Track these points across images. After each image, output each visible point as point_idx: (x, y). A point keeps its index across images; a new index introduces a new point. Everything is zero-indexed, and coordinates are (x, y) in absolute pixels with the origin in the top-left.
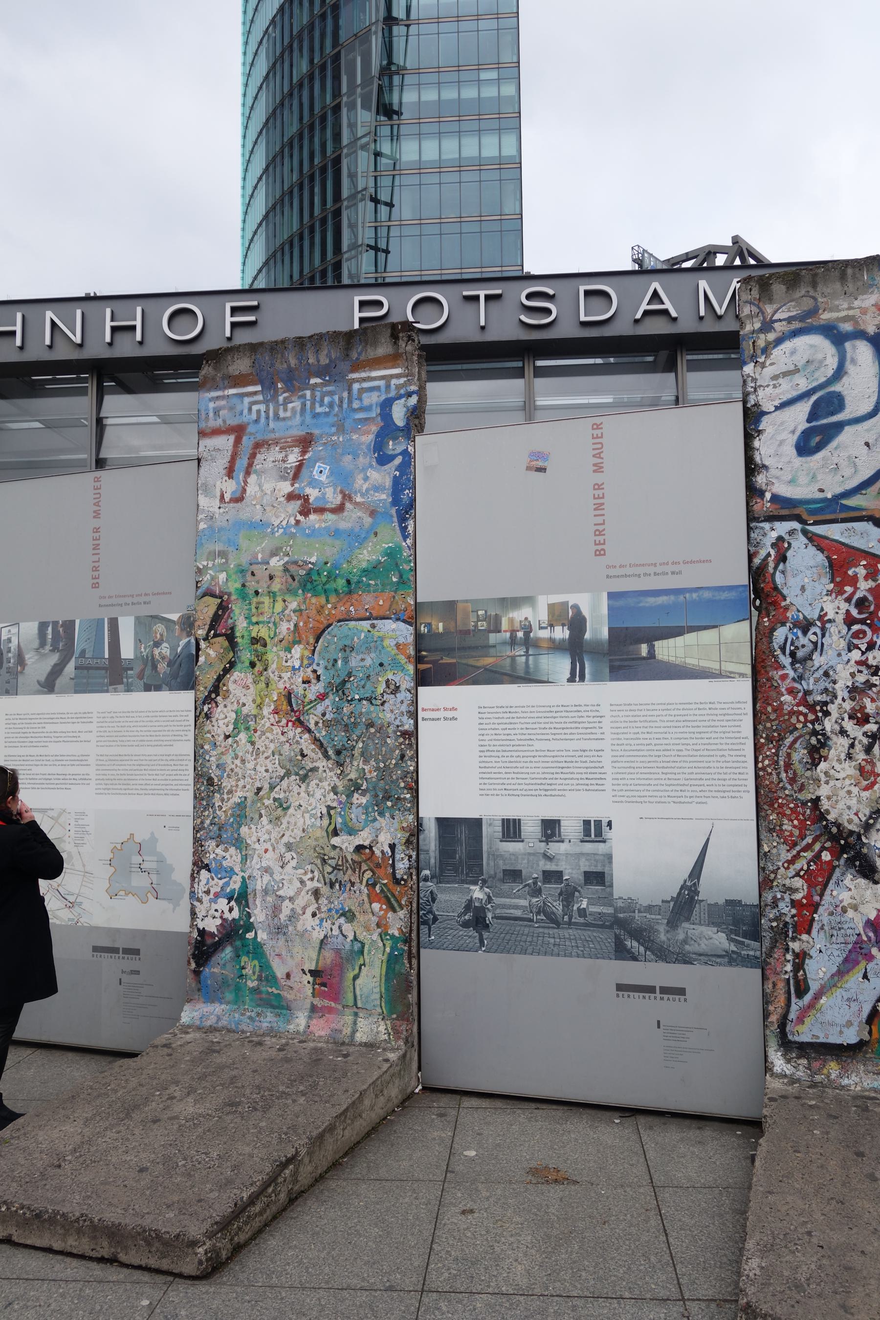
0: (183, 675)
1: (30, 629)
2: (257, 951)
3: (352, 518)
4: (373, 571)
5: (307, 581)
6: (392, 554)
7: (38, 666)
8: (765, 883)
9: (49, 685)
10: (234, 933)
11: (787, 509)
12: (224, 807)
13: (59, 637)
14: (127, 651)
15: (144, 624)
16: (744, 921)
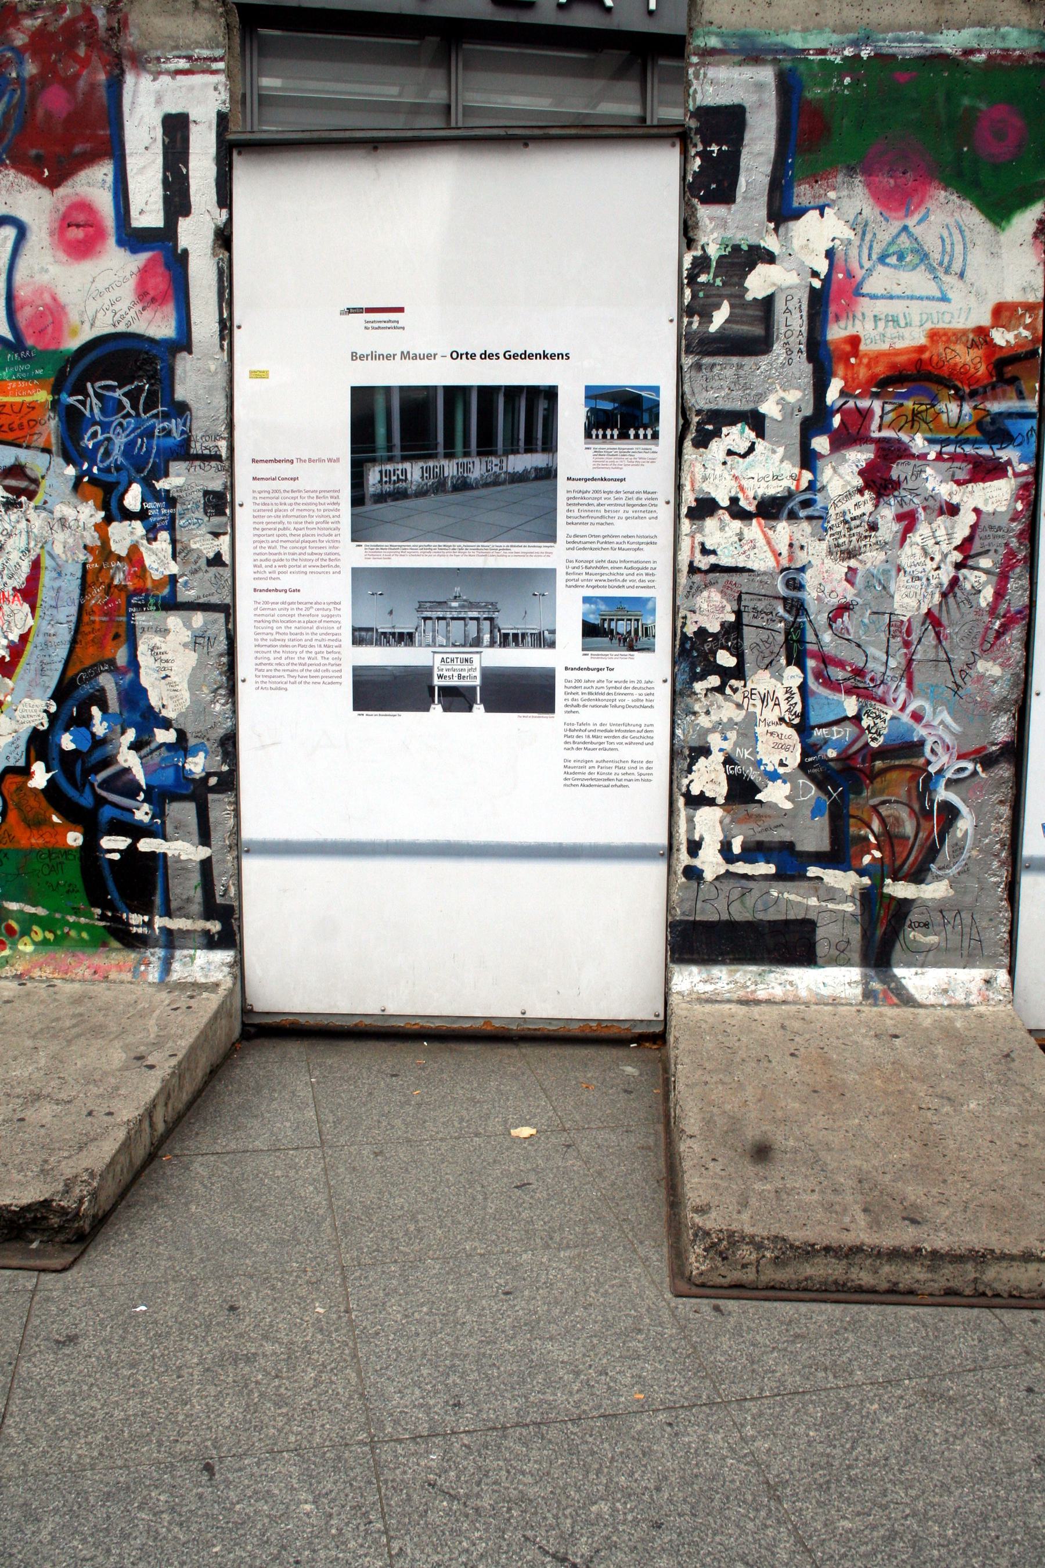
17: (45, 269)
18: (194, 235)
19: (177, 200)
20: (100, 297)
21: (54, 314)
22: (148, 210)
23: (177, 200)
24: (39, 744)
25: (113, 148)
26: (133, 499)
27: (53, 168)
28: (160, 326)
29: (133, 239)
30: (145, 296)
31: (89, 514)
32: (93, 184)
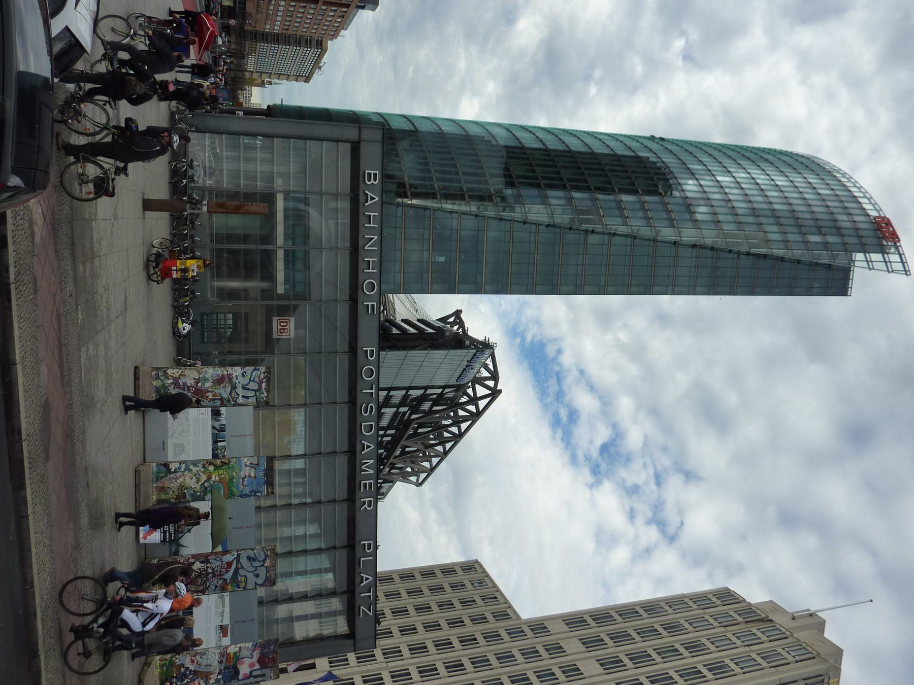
0: (215, 456)
1: (224, 422)
2: (166, 476)
3: (242, 487)
4: (232, 491)
5: (231, 479)
6: (234, 495)
7: (217, 425)
8: (182, 557)
9: (213, 427)
10: (169, 471)
11: (239, 555)
12: (191, 467)
13: (222, 429)
14: (219, 444)
15: (224, 447)
16: (177, 553)
17: (247, 661)
18: (252, 679)
19: (256, 677)
20: (244, 669)
21: (242, 663)
22: (254, 674)
23: (256, 677)
24: (187, 668)
25: (261, 668)
26: (220, 677)
27: (260, 661)
28: (241, 677)
29: (251, 672)
30: (245, 674)
31: (218, 671)
32: (257, 666)
